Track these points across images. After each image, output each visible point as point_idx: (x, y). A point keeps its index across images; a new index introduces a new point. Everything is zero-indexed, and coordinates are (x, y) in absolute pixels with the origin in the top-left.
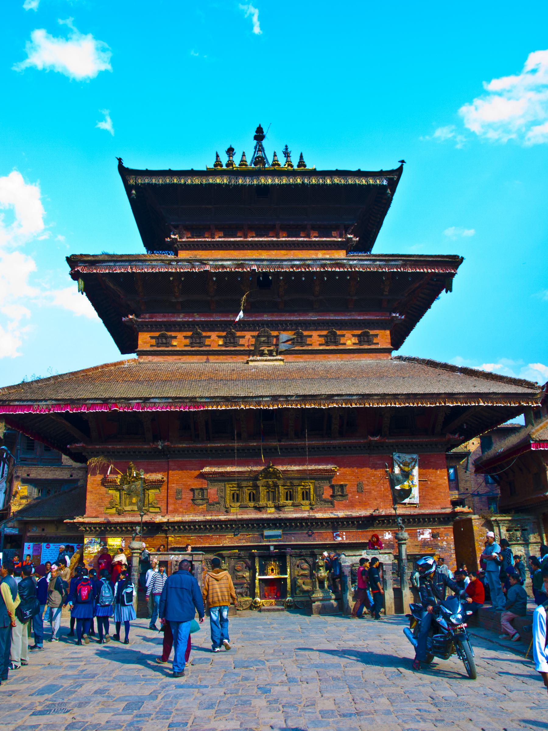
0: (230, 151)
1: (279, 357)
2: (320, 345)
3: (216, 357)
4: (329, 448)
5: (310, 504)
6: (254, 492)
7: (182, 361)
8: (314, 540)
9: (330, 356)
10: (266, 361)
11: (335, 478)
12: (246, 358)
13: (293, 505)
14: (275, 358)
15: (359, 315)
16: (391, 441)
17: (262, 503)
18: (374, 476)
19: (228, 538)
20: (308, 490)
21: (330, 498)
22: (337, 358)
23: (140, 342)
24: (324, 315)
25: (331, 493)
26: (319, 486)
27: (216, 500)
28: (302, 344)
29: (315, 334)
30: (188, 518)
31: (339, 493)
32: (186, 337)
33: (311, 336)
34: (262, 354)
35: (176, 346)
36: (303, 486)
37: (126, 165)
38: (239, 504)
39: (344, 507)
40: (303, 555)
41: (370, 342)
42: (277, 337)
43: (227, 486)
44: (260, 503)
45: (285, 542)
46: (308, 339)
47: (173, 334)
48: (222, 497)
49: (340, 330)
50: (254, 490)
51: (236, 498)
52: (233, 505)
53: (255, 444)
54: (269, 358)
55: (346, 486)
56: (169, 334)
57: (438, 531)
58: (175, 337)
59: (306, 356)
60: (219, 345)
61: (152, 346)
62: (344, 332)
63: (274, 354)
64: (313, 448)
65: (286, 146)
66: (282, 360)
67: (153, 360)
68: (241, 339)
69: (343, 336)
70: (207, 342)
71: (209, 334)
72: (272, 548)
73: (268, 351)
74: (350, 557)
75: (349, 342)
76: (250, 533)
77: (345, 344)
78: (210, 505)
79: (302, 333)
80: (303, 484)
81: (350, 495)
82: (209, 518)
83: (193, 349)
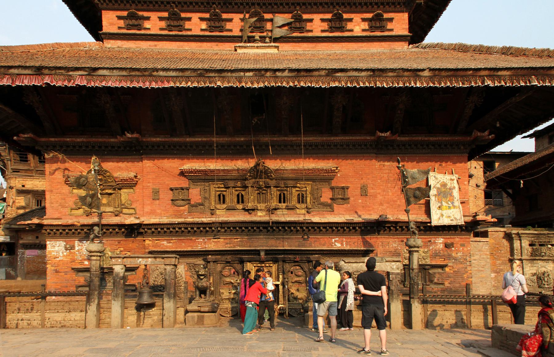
2: (323, 31)
3: (199, 44)
4: (330, 146)
6: (243, 193)
7: (158, 47)
8: (311, 246)
10: (257, 47)
11: (335, 179)
12: (233, 45)
13: (288, 208)
14: (268, 45)
17: (250, 205)
18: (381, 179)
19: (213, 242)
20: (304, 193)
21: (329, 201)
22: (343, 47)
23: (104, 23)
25: (331, 197)
26: (316, 188)
27: (200, 201)
28: (301, 29)
31: (341, 196)
32: (161, 19)
33: (311, 20)
34: (251, 39)
35: (149, 29)
36: (299, 187)
38: (225, 206)
39: (345, 211)
40: (297, 262)
41: (382, 28)
42: (271, 20)
43: (212, 186)
44: (250, 205)
45: (278, 247)
46: (308, 24)
47: (146, 14)
48: (205, 198)
50: (244, 191)
51: (222, 199)
52: (218, 206)
53: (242, 139)
55: (348, 189)
56: (141, 13)
57: (452, 240)
58: (148, 18)
59: (305, 45)
60: (202, 30)
61: (120, 28)
63: (267, 40)
64: (311, 146)
66: (276, 47)
67: (122, 45)
68: (227, 23)
69: (351, 20)
70: (187, 25)
71: (188, 15)
72: (262, 254)
73: (260, 37)
74: (350, 264)
76: (238, 237)
77: (352, 31)
78: (193, 206)
79: (300, 16)
80: (298, 185)
81: (352, 199)
82: (190, 220)
83: (171, 33)
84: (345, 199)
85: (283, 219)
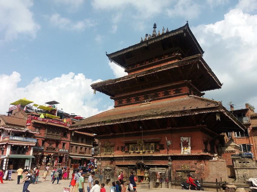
0: (147, 35)
5: (153, 152)
9: (166, 99)
13: (148, 152)
15: (176, 83)
16: (178, 128)
21: (159, 149)
24: (163, 86)
29: (161, 93)
30: (119, 156)
31: (162, 148)
32: (126, 100)
33: (160, 94)
34: (144, 102)
37: (107, 54)
46: (159, 95)
47: (123, 100)
56: (122, 100)
58: (123, 101)
65: (163, 27)
66: (150, 103)
69: (170, 92)
71: (131, 98)
75: (172, 93)
77: (171, 94)
84: (163, 149)
85: (148, 155)
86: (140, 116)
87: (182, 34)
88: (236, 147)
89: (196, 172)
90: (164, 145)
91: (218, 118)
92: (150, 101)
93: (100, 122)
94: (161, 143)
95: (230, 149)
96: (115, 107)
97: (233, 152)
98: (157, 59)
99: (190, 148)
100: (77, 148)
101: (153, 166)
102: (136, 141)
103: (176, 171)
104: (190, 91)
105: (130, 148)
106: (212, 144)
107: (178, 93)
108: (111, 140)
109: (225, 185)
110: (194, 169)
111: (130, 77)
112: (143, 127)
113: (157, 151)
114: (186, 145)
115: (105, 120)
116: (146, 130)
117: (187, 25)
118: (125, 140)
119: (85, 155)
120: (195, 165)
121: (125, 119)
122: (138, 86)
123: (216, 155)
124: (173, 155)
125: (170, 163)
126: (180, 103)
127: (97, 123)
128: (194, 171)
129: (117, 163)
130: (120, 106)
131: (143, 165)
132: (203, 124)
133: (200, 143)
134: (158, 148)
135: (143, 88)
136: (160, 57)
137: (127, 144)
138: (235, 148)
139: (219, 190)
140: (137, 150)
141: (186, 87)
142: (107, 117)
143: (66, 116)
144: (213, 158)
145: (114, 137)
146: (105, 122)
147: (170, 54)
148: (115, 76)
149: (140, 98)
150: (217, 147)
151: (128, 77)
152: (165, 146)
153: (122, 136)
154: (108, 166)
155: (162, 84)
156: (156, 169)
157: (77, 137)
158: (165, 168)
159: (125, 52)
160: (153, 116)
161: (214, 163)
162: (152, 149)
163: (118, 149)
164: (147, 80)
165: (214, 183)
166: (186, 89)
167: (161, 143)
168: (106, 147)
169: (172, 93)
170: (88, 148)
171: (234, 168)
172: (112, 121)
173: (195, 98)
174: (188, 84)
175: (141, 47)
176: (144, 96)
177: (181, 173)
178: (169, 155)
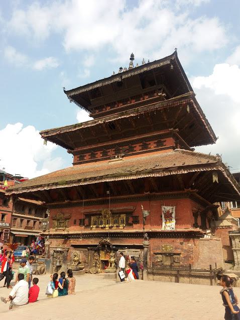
1: (121, 158)
2: (140, 150)
13: (117, 226)
16: (158, 194)
21: (131, 222)
28: (133, 151)
30: (76, 232)
31: (136, 221)
33: (135, 147)
34: (114, 158)
47: (85, 155)
49: (148, 141)
54: (117, 159)
62: (151, 142)
66: (122, 160)
69: (150, 144)
75: (152, 147)
77: (150, 148)
86: (107, 176)
87: (168, 66)
88: (233, 221)
89: (181, 255)
90: (138, 217)
91: (215, 179)
92: (123, 157)
93: (50, 185)
94: (134, 215)
95: (225, 223)
96: (74, 164)
97: (230, 228)
98: (134, 101)
99: (174, 222)
100: (22, 221)
101: (123, 247)
102: (101, 211)
103: (154, 253)
104: (176, 144)
105: (92, 221)
106: (204, 216)
107: (160, 146)
108: (66, 210)
109: (222, 273)
110: (179, 251)
111: (95, 122)
112: (111, 192)
113: (129, 225)
114: (168, 216)
115: (57, 182)
116: (116, 196)
117: (175, 53)
118: (83, 210)
119: (34, 231)
120: (180, 245)
121: (85, 180)
122: (106, 135)
123: (208, 231)
124: (150, 231)
125: (146, 242)
126: (163, 159)
127: (45, 185)
128: (179, 254)
129: (73, 243)
130: (80, 163)
131: (109, 246)
132: (192, 188)
133: (189, 214)
134: (130, 221)
135: (113, 139)
136: (137, 97)
137: (89, 216)
138: (232, 222)
139: (213, 280)
140: (101, 224)
141: (171, 138)
142: (61, 177)
143: (9, 177)
144: (205, 236)
145: (69, 205)
146: (57, 184)
147: (151, 94)
148: (77, 120)
149: (109, 152)
150: (209, 222)
151: (93, 122)
152: (140, 219)
153: (79, 204)
154: (61, 246)
155: (139, 134)
156: (126, 250)
157: (20, 207)
158: (139, 250)
159: (90, 88)
160: (125, 175)
161: (206, 243)
162: (123, 223)
163: (75, 223)
164: (119, 128)
165: (208, 271)
166: (170, 141)
167: (134, 215)
168: (58, 220)
169: (153, 146)
170: (38, 222)
171: (233, 249)
172: (67, 183)
173: (183, 152)
174: (174, 134)
175: (112, 81)
176: (114, 149)
177: (161, 256)
178: (145, 230)
